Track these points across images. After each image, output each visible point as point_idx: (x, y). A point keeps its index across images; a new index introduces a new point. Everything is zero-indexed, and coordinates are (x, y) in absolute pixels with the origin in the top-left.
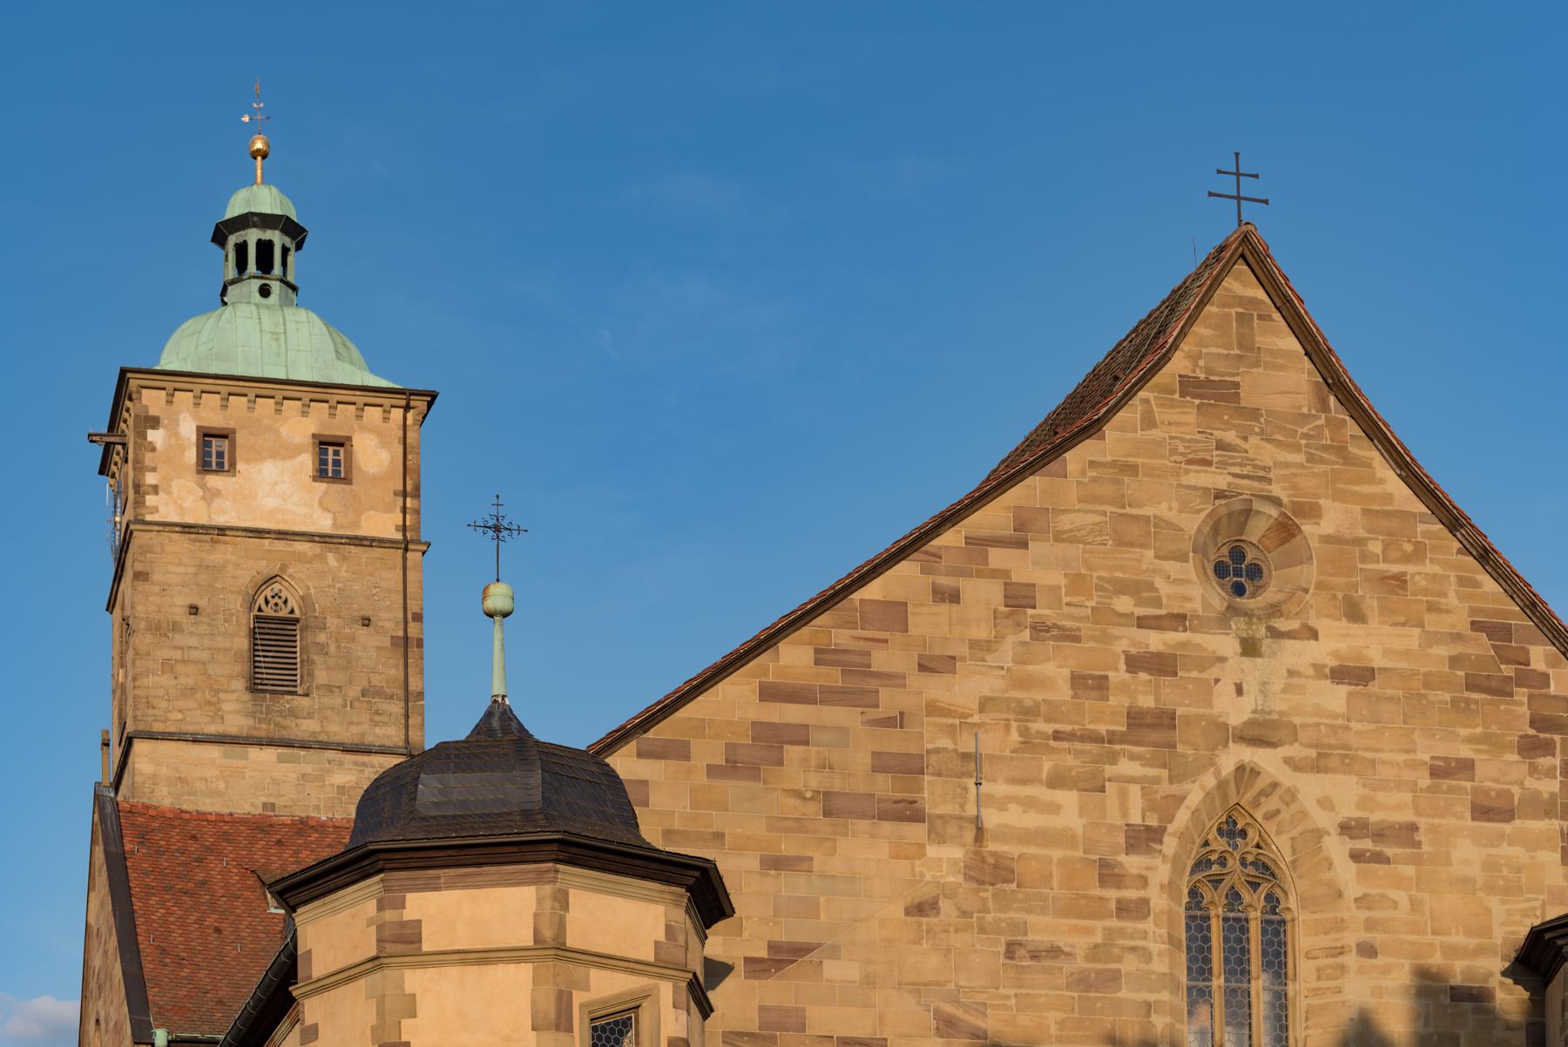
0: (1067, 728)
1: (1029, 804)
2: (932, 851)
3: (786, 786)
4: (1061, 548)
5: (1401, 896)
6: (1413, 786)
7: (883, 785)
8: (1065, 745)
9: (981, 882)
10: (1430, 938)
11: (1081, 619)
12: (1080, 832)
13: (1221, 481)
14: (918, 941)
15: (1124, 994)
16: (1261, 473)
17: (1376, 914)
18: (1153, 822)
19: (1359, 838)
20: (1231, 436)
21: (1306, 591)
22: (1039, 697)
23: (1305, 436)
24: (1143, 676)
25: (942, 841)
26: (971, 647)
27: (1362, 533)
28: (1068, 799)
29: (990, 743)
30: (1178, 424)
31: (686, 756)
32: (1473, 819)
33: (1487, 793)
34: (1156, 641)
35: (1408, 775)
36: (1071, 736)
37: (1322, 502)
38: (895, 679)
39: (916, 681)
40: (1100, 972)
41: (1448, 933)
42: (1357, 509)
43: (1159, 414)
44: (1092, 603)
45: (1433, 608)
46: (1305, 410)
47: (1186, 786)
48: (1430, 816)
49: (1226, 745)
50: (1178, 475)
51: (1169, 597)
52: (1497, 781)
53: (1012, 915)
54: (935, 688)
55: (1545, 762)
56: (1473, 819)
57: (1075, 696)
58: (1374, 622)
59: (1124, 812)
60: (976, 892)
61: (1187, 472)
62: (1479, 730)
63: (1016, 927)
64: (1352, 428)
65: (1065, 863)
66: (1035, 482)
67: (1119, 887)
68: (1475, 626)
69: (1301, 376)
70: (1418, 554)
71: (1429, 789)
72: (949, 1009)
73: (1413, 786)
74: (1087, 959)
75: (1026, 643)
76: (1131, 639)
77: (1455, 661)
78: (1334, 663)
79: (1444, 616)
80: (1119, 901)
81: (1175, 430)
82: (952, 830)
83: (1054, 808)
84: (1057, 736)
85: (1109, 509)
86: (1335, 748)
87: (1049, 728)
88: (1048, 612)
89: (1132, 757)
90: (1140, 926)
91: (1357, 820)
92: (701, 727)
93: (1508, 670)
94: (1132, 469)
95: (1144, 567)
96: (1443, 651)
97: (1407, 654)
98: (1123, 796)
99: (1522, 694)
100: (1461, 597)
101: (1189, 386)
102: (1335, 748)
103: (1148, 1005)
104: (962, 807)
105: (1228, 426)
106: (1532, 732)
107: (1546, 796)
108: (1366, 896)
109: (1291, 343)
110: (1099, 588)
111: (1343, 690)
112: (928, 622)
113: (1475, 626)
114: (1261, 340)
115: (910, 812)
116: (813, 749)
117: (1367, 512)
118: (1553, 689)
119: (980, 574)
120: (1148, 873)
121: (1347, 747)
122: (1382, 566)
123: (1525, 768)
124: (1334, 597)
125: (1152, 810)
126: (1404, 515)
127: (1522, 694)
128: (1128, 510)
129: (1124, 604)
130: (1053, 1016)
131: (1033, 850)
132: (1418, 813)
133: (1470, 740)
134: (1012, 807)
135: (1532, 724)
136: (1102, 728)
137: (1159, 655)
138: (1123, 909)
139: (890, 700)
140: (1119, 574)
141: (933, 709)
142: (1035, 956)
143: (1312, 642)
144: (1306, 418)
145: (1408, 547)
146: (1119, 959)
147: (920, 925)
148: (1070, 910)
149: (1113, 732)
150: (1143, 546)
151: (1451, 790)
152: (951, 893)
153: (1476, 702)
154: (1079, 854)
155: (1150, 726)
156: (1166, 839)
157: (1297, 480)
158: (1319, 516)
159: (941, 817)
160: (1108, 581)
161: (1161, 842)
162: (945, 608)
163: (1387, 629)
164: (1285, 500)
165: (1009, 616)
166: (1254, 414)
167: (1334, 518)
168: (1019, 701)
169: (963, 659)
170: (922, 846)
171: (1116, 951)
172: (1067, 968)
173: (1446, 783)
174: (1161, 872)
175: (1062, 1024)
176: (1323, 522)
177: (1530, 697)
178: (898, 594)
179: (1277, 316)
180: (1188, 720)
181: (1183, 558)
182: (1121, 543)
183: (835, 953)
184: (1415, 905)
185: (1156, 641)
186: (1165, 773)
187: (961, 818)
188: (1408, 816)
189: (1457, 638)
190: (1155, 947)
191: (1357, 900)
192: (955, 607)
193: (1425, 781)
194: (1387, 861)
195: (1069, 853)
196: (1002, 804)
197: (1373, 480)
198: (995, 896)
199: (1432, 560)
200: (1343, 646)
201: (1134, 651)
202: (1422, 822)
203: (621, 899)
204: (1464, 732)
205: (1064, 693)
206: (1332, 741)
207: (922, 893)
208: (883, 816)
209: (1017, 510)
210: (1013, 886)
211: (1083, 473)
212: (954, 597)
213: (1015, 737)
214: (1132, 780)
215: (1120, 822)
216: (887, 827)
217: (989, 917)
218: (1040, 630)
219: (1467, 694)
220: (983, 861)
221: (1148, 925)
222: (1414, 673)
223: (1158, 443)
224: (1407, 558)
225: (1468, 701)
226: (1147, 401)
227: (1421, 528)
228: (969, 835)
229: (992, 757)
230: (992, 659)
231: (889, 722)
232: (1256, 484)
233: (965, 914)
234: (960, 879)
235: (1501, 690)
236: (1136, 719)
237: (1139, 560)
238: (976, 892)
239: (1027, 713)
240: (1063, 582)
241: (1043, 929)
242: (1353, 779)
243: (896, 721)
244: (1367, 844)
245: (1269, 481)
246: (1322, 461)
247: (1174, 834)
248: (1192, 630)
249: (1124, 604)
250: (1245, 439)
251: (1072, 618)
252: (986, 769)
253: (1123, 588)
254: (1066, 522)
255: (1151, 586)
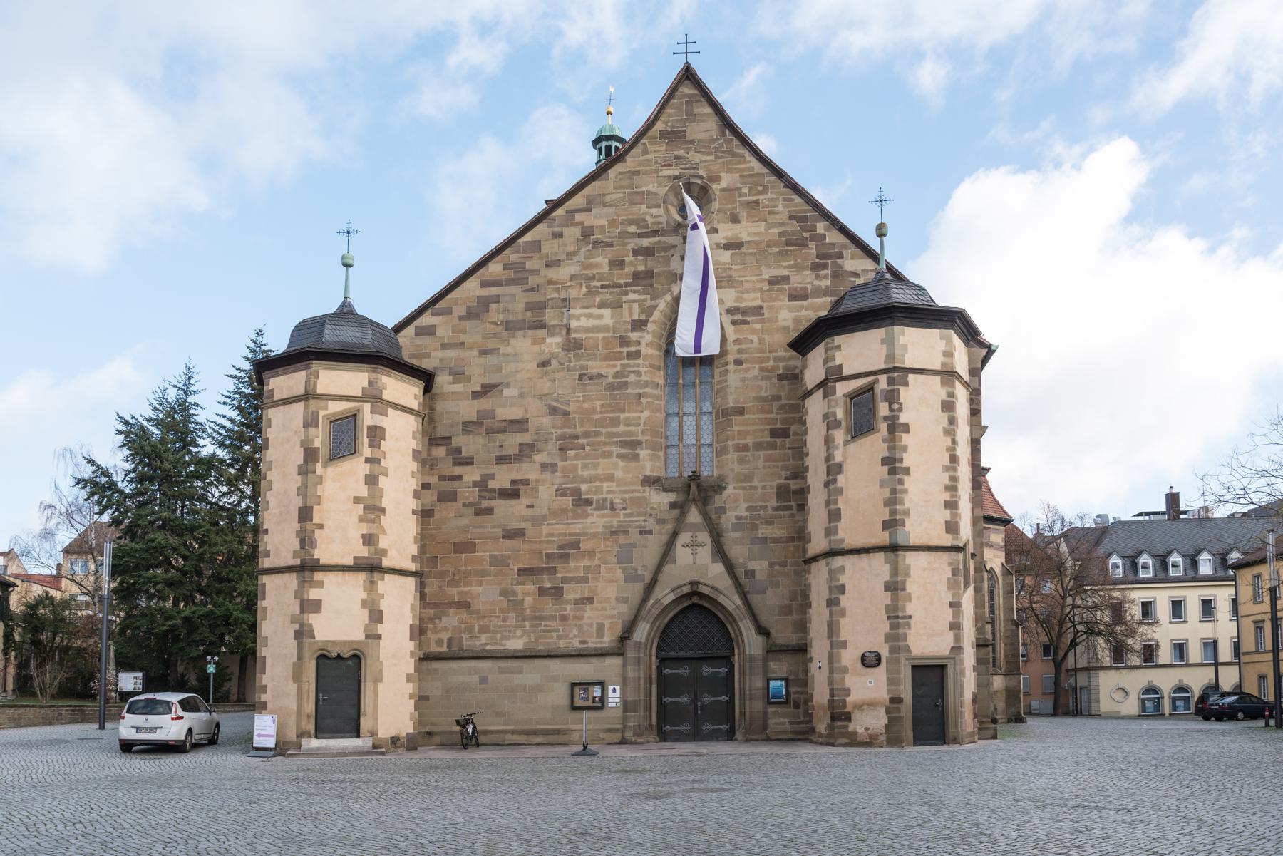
0: (607, 283)
1: (589, 316)
2: (549, 340)
3: (490, 320)
4: (605, 210)
5: (755, 338)
6: (761, 290)
7: (530, 316)
8: (606, 290)
9: (569, 351)
10: (768, 354)
11: (613, 238)
12: (611, 325)
13: (675, 172)
14: (542, 378)
15: (628, 391)
16: (694, 166)
17: (743, 346)
18: (643, 317)
19: (734, 314)
20: (681, 153)
21: (713, 213)
22: (595, 272)
23: (715, 148)
24: (640, 258)
25: (551, 334)
26: (567, 255)
27: (739, 185)
28: (607, 312)
29: (573, 293)
30: (658, 151)
31: (451, 313)
32: (789, 301)
33: (795, 289)
34: (646, 242)
35: (759, 285)
36: (608, 286)
37: (721, 174)
38: (535, 272)
39: (544, 272)
40: (618, 383)
41: (776, 351)
42: (737, 175)
43: (650, 148)
44: (619, 230)
45: (770, 213)
46: (715, 137)
47: (658, 301)
48: (769, 302)
49: (676, 282)
50: (657, 172)
51: (652, 223)
52: (800, 283)
53: (582, 363)
54: (553, 274)
55: (823, 272)
56: (789, 301)
57: (610, 269)
58: (744, 222)
59: (631, 315)
60: (567, 355)
61: (662, 170)
62: (792, 262)
63: (583, 367)
64: (736, 142)
65: (604, 338)
66: (596, 184)
67: (628, 346)
68: (791, 218)
69: (713, 124)
70: (765, 190)
71: (768, 290)
72: (554, 404)
73: (761, 290)
74: (613, 377)
75: (588, 251)
76: (633, 244)
77: (781, 234)
78: (726, 242)
79: (778, 216)
80: (627, 352)
81: (656, 154)
82: (557, 330)
83: (600, 317)
84: (602, 287)
85: (627, 191)
86: (725, 277)
87: (599, 284)
88: (599, 236)
89: (635, 292)
90: (637, 362)
91: (735, 307)
92: (457, 301)
93: (806, 235)
94: (637, 173)
95: (641, 212)
96: (776, 231)
97: (759, 234)
98: (630, 308)
99: (812, 245)
100: (784, 206)
101: (663, 134)
102: (725, 277)
103: (640, 394)
104: (562, 321)
105: (680, 149)
106: (817, 260)
107: (823, 287)
108: (738, 339)
109: (708, 110)
110: (622, 224)
111: (729, 253)
112: (549, 247)
113: (791, 218)
114: (696, 111)
115: (540, 325)
116: (501, 304)
117: (742, 176)
118: (827, 241)
119: (571, 225)
120: (641, 340)
121: (731, 277)
122: (748, 198)
123: (814, 276)
124: (726, 214)
125: (642, 313)
126: (758, 174)
127: (812, 245)
128: (635, 190)
129: (632, 229)
130: (598, 403)
131: (591, 335)
132: (763, 301)
133: (788, 267)
134: (582, 318)
135: (817, 257)
136: (622, 281)
137: (647, 248)
138: (630, 356)
139: (533, 280)
140: (630, 217)
141: (551, 282)
142: (591, 378)
143: (716, 234)
144: (714, 141)
145: (760, 188)
146: (627, 377)
147: (543, 371)
148: (607, 358)
149: (626, 283)
150: (641, 204)
151: (779, 290)
152: (556, 356)
153: (791, 250)
154: (611, 334)
155: (643, 278)
156: (649, 324)
157: (711, 167)
158: (720, 181)
159: (553, 326)
160: (625, 220)
161: (647, 326)
162: (556, 241)
163: (751, 224)
164: (705, 176)
165: (583, 240)
166: (692, 142)
167: (727, 180)
168: (587, 274)
169: (563, 260)
170: (544, 339)
171: (626, 373)
172: (605, 382)
173: (776, 287)
174: (648, 338)
175: (602, 406)
176: (721, 183)
177: (817, 245)
178: (538, 238)
179: (703, 100)
180: (659, 274)
181: (659, 206)
182: (632, 203)
183: (508, 385)
184: (761, 341)
185: (646, 242)
186: (649, 297)
187: (561, 325)
188: (758, 303)
189: (782, 224)
190: (642, 370)
191: (734, 341)
192: (561, 240)
193: (766, 287)
194: (748, 323)
195: (606, 335)
196: (578, 318)
197: (745, 162)
198: (574, 356)
199: (771, 193)
200: (729, 234)
201: (636, 248)
202: (765, 305)
203: (345, 372)
204: (785, 264)
205: (606, 269)
206: (724, 275)
207: (544, 358)
208: (529, 328)
209: (588, 196)
210: (582, 351)
211: (616, 178)
212: (560, 235)
213: (584, 289)
214: (634, 301)
215: (629, 319)
216: (530, 332)
217: (572, 365)
218: (597, 244)
219: (786, 248)
220: (570, 341)
221: (640, 361)
222: (761, 242)
223: (649, 160)
224: (760, 193)
225: (787, 251)
226: (645, 144)
227: (766, 179)
228: (564, 332)
229: (574, 299)
230: (575, 259)
231: (533, 290)
232: (692, 171)
233: (561, 364)
234: (560, 350)
235: (803, 244)
236: (637, 276)
237: (640, 210)
238: (567, 355)
239: (592, 278)
240: (606, 223)
241: (595, 367)
242: (734, 289)
243: (536, 289)
244: (739, 317)
245: (698, 169)
246: (722, 157)
247: (652, 322)
248: (662, 236)
249: (632, 229)
250: (688, 153)
251: (610, 237)
252: (571, 303)
253: (632, 222)
254: (608, 198)
255: (644, 220)
